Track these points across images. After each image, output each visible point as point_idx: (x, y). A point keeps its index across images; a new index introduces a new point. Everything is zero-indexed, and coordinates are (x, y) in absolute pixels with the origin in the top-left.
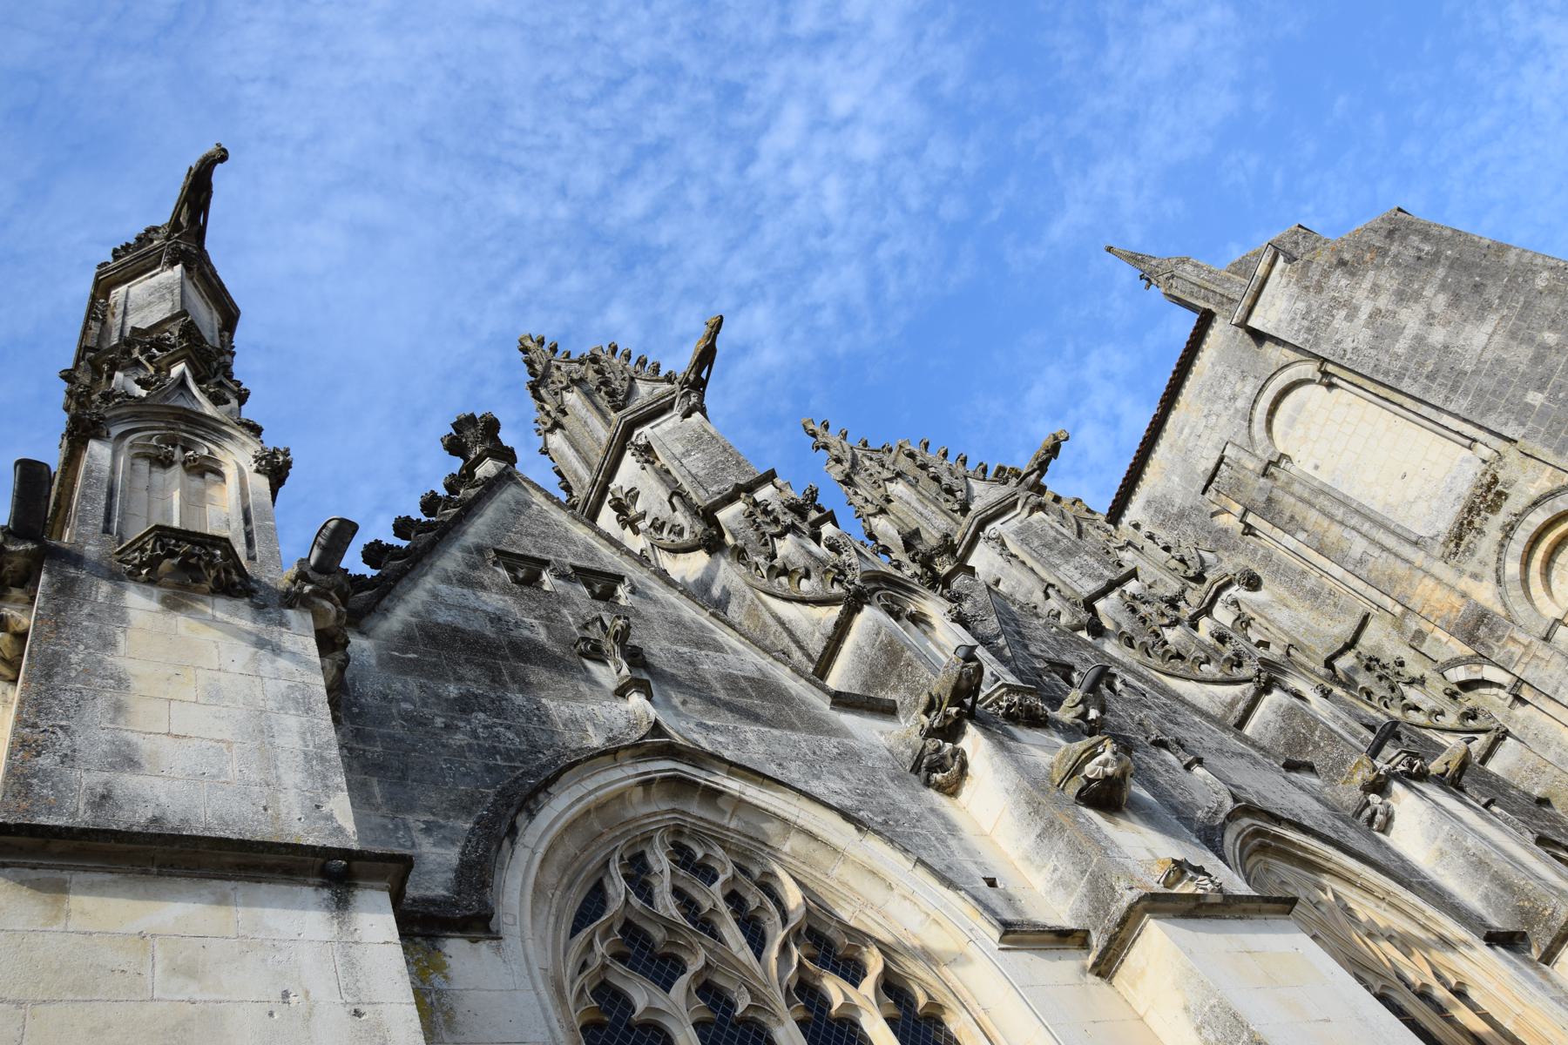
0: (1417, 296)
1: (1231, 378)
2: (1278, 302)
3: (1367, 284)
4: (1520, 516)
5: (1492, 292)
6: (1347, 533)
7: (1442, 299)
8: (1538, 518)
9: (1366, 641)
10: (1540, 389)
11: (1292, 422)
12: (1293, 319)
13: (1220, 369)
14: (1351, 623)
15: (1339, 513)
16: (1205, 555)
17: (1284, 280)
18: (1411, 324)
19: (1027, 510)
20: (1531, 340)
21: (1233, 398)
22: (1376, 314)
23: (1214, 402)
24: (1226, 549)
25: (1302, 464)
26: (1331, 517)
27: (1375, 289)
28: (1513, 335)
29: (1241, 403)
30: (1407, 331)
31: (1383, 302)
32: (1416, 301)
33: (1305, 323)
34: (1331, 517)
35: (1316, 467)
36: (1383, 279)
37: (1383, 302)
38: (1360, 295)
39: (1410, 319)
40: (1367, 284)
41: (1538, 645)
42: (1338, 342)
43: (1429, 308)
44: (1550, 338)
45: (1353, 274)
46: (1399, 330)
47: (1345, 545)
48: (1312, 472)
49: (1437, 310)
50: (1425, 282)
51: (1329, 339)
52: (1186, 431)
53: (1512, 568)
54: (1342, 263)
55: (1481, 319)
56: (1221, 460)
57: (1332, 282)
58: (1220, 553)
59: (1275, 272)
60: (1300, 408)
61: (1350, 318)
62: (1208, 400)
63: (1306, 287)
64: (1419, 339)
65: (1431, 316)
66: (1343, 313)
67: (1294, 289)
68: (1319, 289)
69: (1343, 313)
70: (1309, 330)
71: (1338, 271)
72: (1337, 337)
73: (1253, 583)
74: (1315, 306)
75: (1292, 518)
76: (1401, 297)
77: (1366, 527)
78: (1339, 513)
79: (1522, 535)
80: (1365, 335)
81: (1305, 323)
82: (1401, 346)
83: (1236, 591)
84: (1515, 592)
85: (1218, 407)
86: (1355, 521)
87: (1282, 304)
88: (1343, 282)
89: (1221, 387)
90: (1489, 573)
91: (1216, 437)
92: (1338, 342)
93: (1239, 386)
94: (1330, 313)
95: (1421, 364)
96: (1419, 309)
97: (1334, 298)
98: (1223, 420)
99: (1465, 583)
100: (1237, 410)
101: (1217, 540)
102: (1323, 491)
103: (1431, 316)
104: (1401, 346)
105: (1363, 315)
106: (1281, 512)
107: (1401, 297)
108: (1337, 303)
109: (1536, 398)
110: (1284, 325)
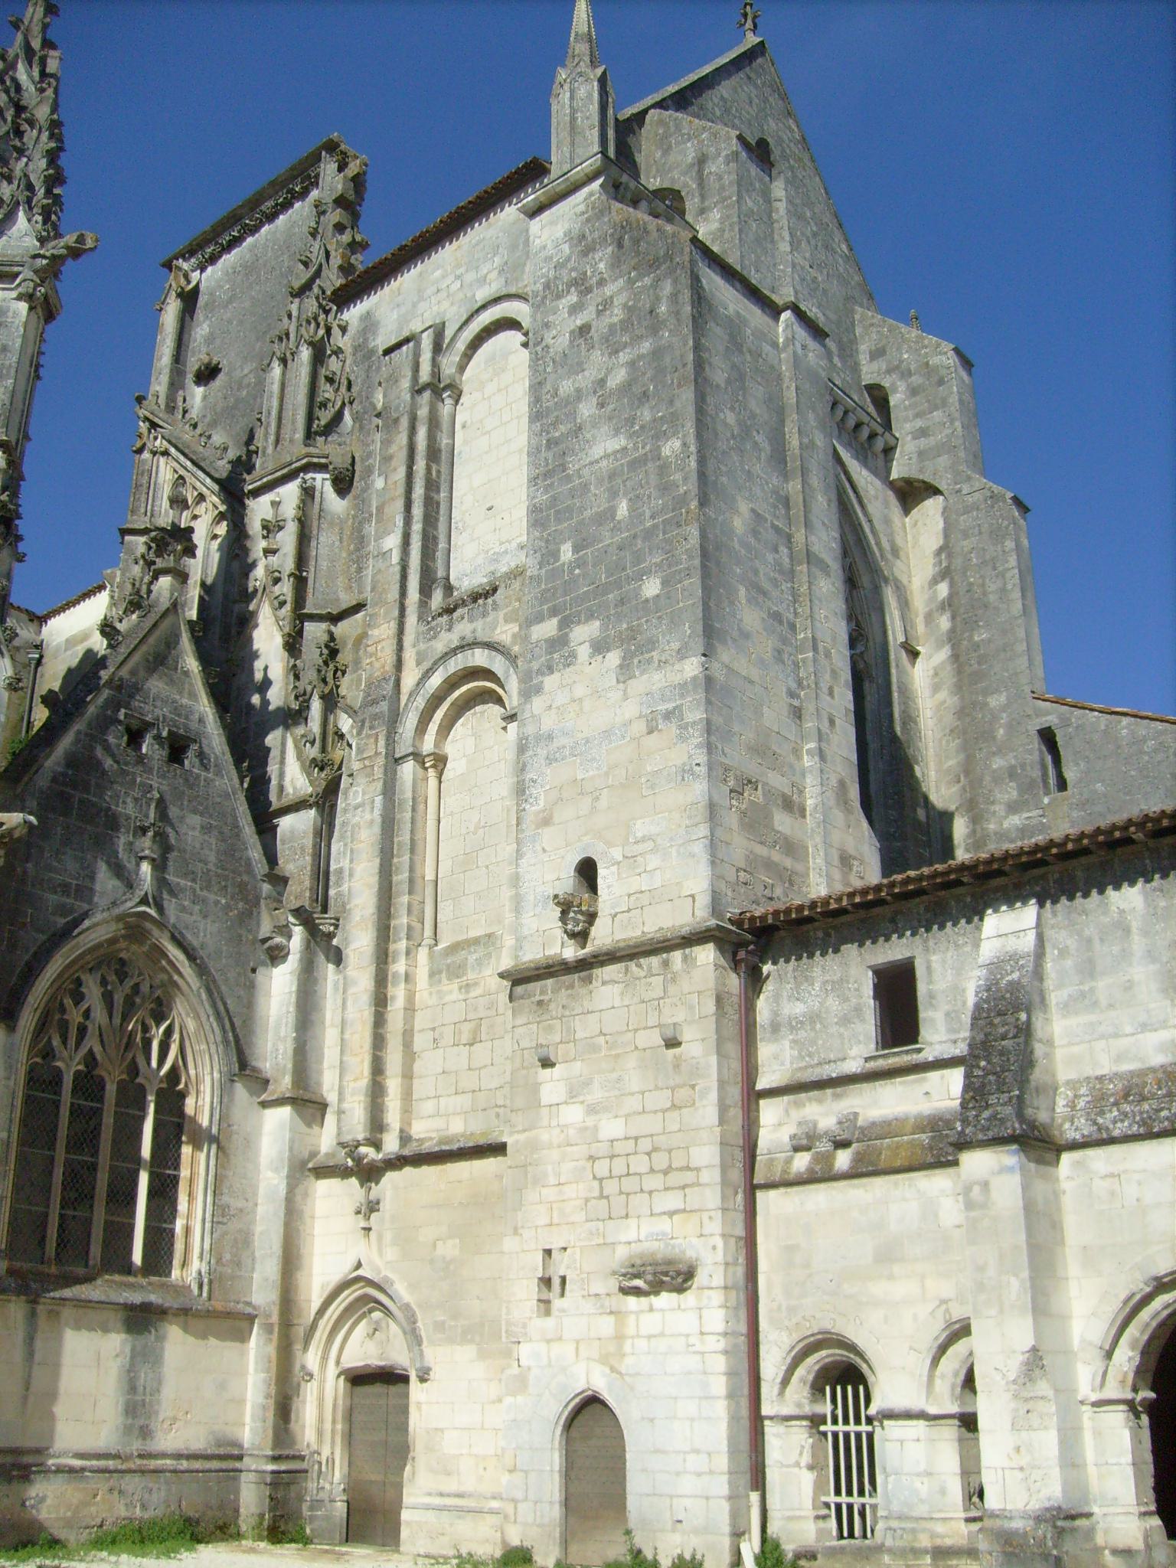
4: (474, 644)
5: (646, 414)
6: (399, 521)
7: (618, 378)
8: (480, 658)
9: (341, 629)
10: (576, 549)
14: (346, 600)
16: (347, 417)
19: (14, 294)
20: (614, 494)
28: (612, 475)
29: (482, 295)
41: (381, 761)
44: (623, 509)
53: (436, 680)
55: (617, 432)
57: (598, 255)
59: (585, 191)
61: (574, 310)
63: (584, 236)
65: (602, 382)
68: (585, 253)
73: (343, 484)
77: (417, 527)
78: (419, 491)
79: (455, 665)
82: (566, 387)
83: (322, 481)
84: (420, 702)
86: (417, 511)
87: (559, 231)
90: (426, 665)
99: (409, 655)
103: (602, 382)
109: (567, 553)
110: (543, 255)
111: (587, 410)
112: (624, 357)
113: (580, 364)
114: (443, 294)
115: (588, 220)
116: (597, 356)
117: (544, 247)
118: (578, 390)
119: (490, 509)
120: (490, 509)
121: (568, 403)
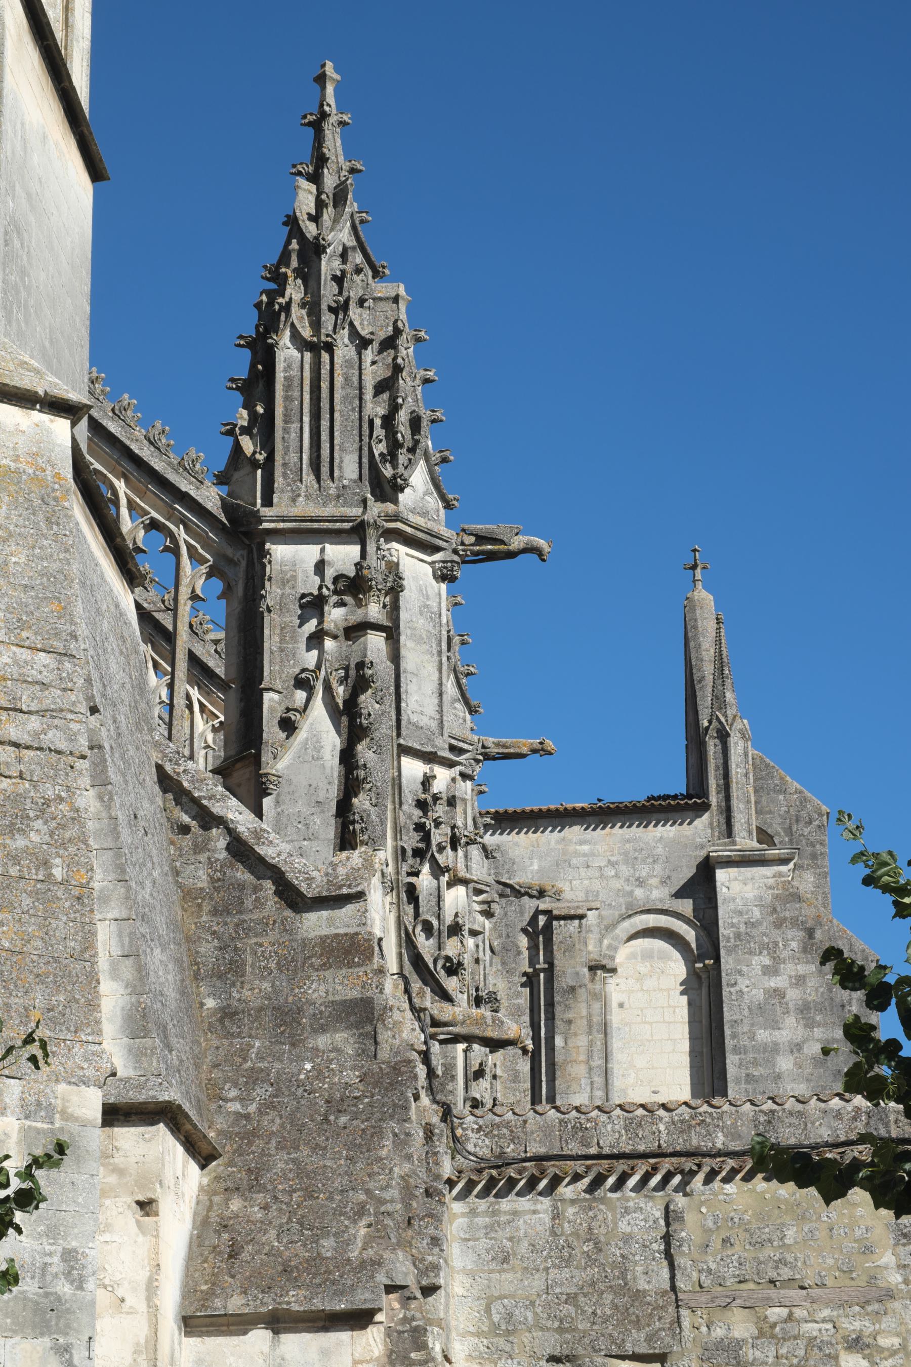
0: (810, 1025)
1: (658, 868)
2: (749, 887)
3: (802, 969)
11: (647, 956)
12: (740, 913)
13: (660, 850)
15: (598, 1062)
17: (771, 881)
18: (784, 1033)
21: (641, 882)
22: (779, 993)
23: (626, 862)
24: (503, 963)
25: (616, 989)
26: (590, 1056)
27: (800, 980)
30: (777, 1033)
31: (793, 995)
32: (806, 1026)
33: (743, 928)
34: (590, 1056)
35: (621, 1005)
36: (812, 982)
37: (793, 995)
38: (790, 969)
39: (790, 1029)
40: (802, 969)
42: (740, 972)
43: (804, 1042)
45: (805, 950)
46: (775, 1025)
47: (574, 1087)
48: (614, 1005)
49: (806, 1050)
50: (825, 1025)
51: (738, 961)
52: (586, 848)
54: (810, 933)
56: (581, 917)
57: (790, 934)
58: (496, 960)
60: (663, 957)
62: (626, 854)
63: (775, 909)
64: (774, 1049)
66: (767, 961)
67: (768, 897)
68: (779, 924)
69: (767, 961)
70: (738, 936)
71: (802, 934)
72: (745, 969)
74: (762, 929)
75: (570, 1022)
76: (804, 1009)
80: (758, 995)
81: (743, 928)
82: (763, 1035)
85: (625, 870)
88: (794, 945)
89: (644, 861)
91: (596, 885)
92: (740, 972)
93: (654, 881)
94: (763, 946)
95: (755, 1063)
96: (800, 1033)
97: (776, 944)
98: (617, 884)
100: (631, 893)
101: (505, 949)
102: (605, 1029)
104: (763, 1035)
105: (774, 982)
106: (568, 1007)
107: (804, 1009)
108: (772, 949)
110: (732, 906)
111: (785, 1063)
112: (818, 1032)
113: (777, 1022)
114: (592, 872)
115: (776, 897)
116: (790, 1021)
117: (734, 899)
118: (776, 1044)
119: (654, 1092)
120: (654, 1092)
121: (765, 1051)
